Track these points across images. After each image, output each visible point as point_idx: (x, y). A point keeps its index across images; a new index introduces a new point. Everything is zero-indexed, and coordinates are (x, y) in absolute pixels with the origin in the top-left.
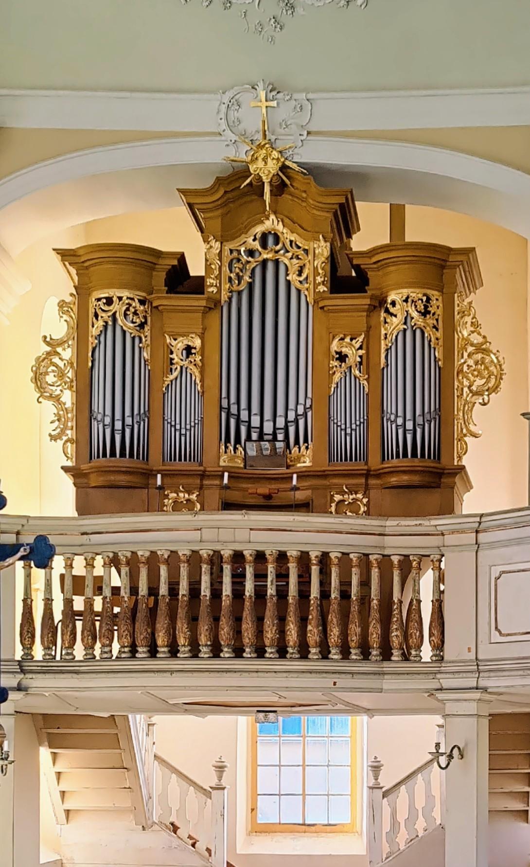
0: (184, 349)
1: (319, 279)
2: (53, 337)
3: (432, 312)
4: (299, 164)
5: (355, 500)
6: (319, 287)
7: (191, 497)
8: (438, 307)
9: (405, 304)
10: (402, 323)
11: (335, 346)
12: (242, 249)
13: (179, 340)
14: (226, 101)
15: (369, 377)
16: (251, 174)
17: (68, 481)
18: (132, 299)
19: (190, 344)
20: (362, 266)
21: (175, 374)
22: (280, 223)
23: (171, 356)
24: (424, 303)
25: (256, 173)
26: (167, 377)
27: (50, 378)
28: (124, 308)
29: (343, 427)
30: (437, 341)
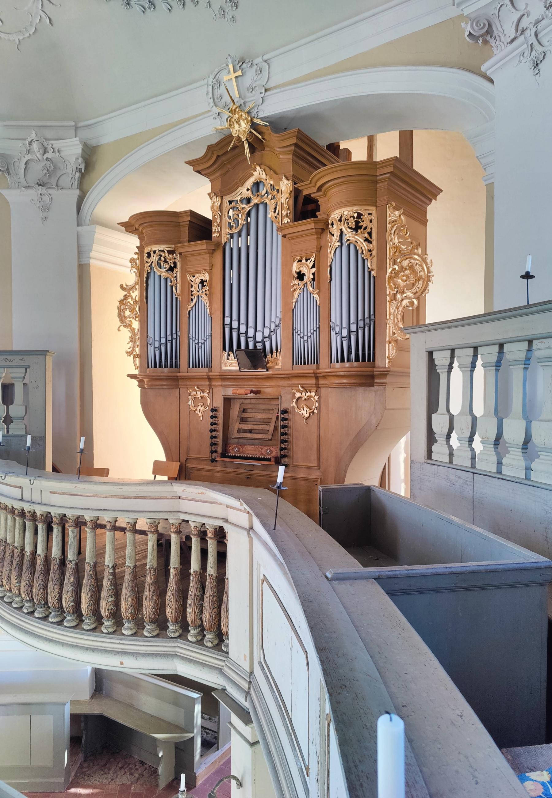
0: (200, 283)
1: (284, 213)
2: (128, 284)
3: (364, 226)
4: (262, 119)
5: (309, 397)
6: (284, 220)
7: (204, 394)
8: (371, 221)
9: (339, 223)
10: (337, 241)
11: (295, 267)
12: (238, 199)
13: (196, 276)
14: (210, 82)
15: (319, 291)
16: (234, 137)
17: (135, 382)
18: (163, 251)
19: (203, 278)
20: (312, 196)
21: (194, 301)
22: (264, 172)
23: (191, 289)
24: (355, 220)
25: (237, 135)
26: (189, 305)
27: (127, 313)
28: (157, 258)
29: (302, 335)
30: (369, 253)
